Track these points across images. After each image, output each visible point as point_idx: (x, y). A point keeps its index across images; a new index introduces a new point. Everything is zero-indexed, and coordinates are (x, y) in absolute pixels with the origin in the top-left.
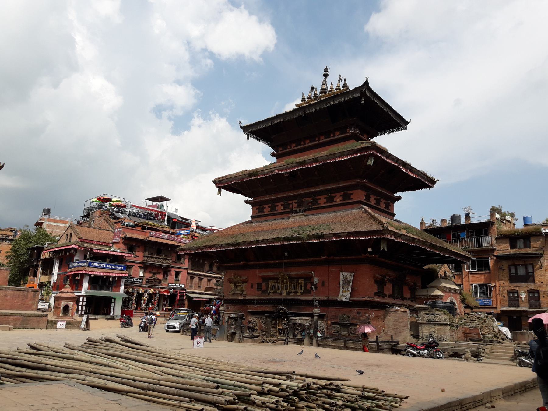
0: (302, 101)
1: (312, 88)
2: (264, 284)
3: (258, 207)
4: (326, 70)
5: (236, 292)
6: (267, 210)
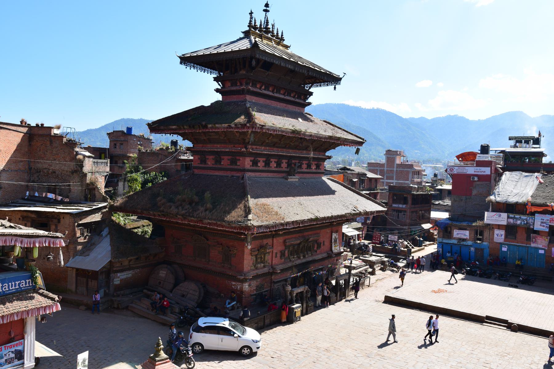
0: (248, 26)
2: (286, 252)
4: (267, 5)
6: (261, 164)
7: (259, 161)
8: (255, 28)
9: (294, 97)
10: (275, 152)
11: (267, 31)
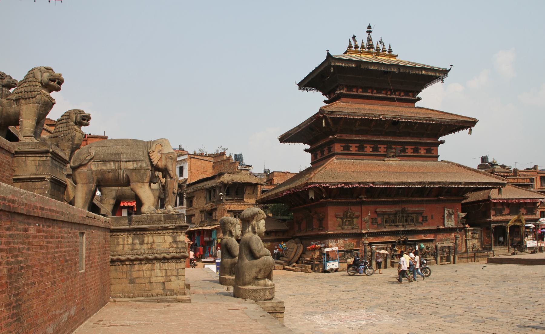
1: (354, 37)
2: (379, 219)
3: (344, 145)
5: (346, 227)
6: (353, 149)
7: (351, 147)
8: (357, 47)
9: (399, 95)
10: (369, 138)
11: (370, 47)
